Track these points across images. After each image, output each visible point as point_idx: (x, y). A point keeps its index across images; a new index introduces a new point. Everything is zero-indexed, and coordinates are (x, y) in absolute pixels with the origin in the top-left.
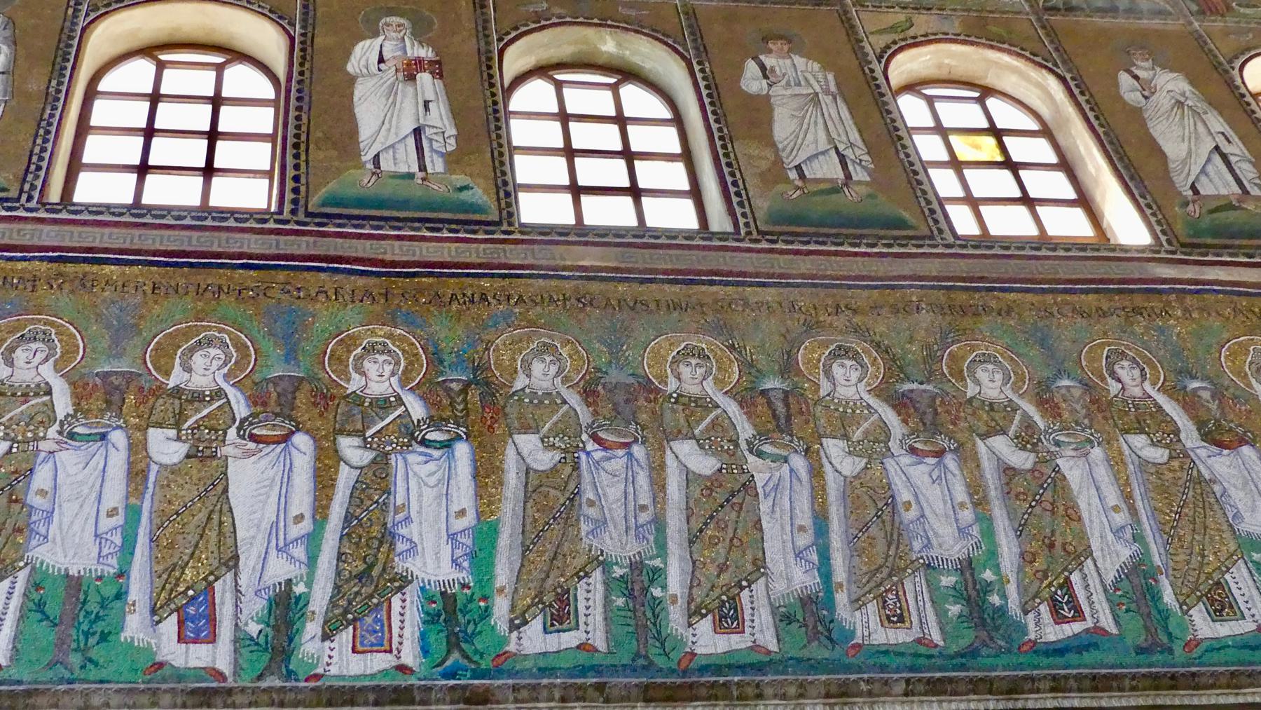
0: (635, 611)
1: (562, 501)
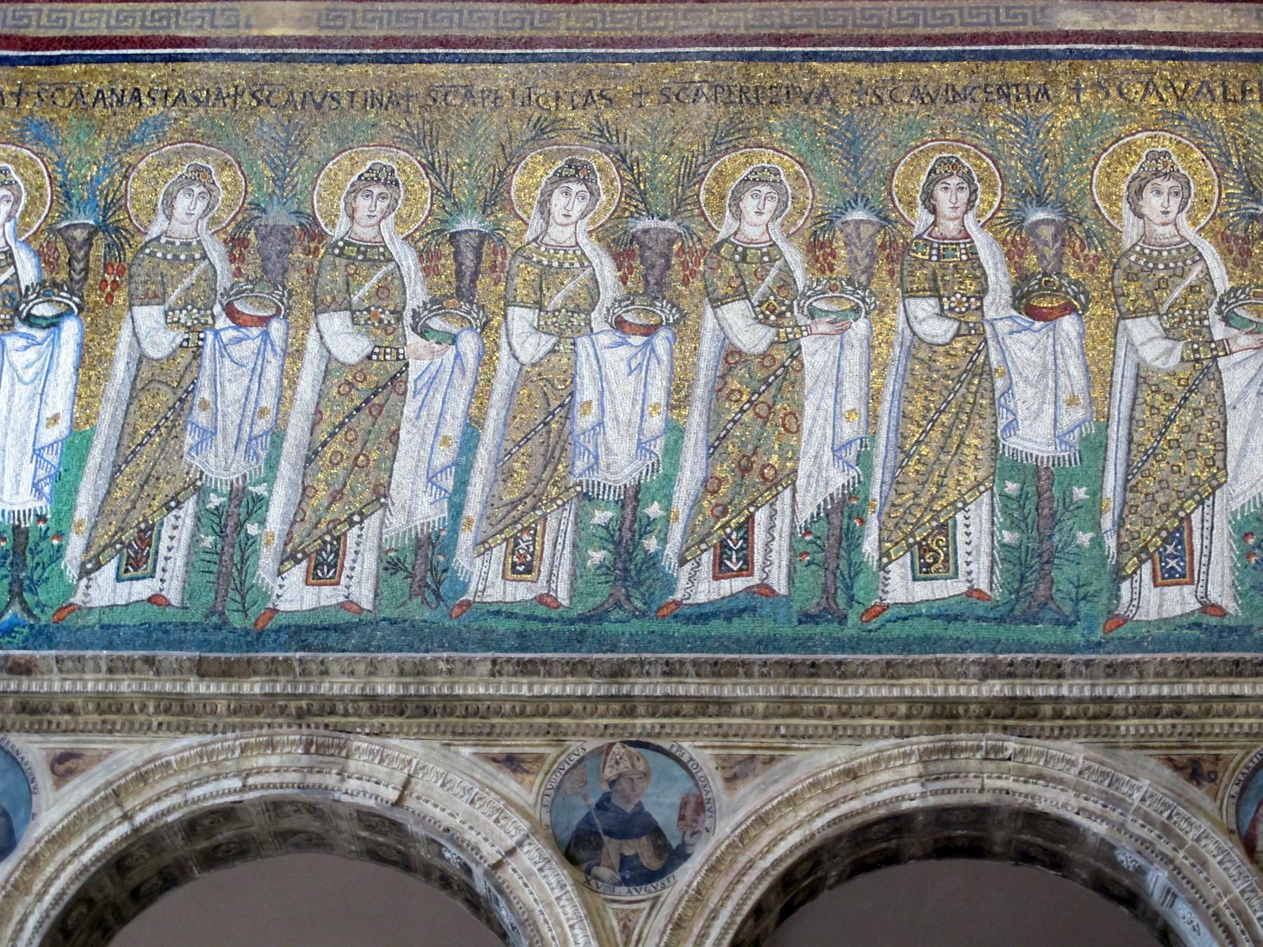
0: (220, 555)
1: (171, 404)
